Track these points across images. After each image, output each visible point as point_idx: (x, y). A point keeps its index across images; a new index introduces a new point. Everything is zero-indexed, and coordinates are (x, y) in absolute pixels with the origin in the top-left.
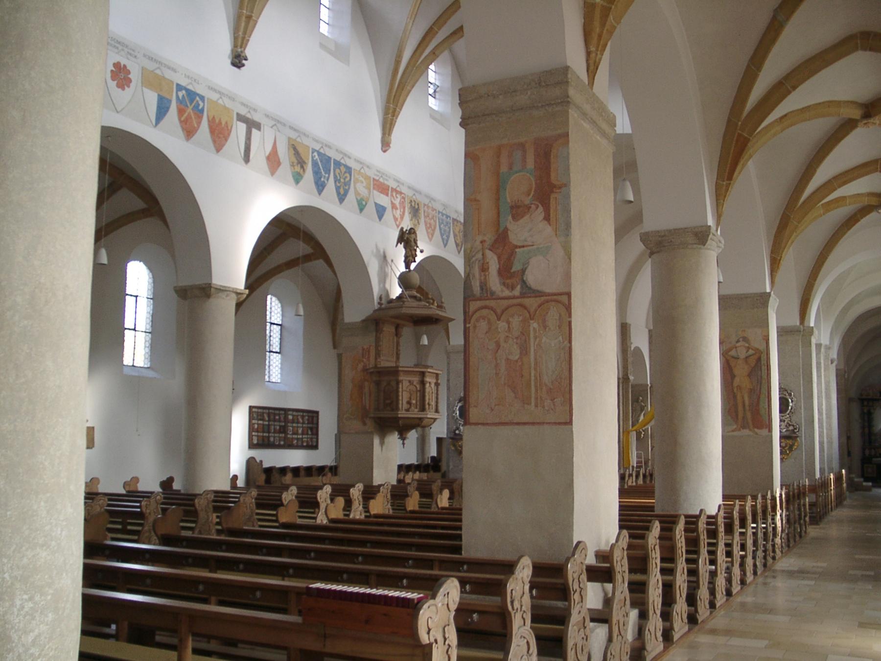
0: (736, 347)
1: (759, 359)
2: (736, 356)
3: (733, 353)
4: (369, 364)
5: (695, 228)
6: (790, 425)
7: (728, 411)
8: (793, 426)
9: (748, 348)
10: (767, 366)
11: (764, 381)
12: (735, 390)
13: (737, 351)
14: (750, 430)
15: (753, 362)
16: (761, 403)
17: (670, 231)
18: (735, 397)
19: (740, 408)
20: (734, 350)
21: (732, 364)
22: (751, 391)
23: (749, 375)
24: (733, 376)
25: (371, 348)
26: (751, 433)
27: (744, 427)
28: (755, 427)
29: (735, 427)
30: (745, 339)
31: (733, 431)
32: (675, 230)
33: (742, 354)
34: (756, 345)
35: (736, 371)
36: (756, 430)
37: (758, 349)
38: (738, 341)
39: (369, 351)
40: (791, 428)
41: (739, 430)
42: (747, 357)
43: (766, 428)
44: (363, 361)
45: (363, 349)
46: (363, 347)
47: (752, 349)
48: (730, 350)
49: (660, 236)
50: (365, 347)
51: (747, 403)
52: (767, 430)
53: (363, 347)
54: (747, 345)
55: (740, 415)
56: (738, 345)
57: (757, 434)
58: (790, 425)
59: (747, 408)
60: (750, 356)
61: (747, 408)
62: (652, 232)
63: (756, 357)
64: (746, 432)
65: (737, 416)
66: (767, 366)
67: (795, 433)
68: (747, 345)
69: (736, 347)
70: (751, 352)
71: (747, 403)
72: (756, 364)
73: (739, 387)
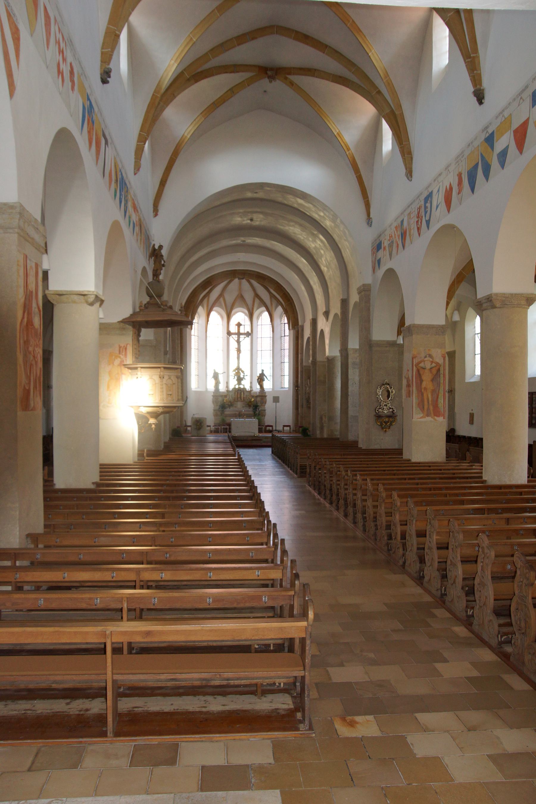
0: (424, 361)
1: (439, 370)
2: (424, 367)
3: (422, 365)
4: (126, 360)
5: (528, 294)
6: (390, 408)
7: (418, 405)
8: (392, 409)
9: (432, 362)
10: (444, 375)
11: (441, 385)
12: (423, 390)
13: (424, 363)
14: (432, 417)
15: (434, 371)
16: (439, 400)
17: (512, 294)
18: (422, 395)
19: (426, 403)
20: (423, 363)
21: (421, 372)
22: (433, 391)
23: (432, 380)
24: (422, 381)
25: (128, 345)
26: (432, 419)
27: (428, 415)
28: (435, 415)
29: (422, 415)
30: (430, 356)
31: (421, 418)
32: (516, 294)
33: (428, 366)
34: (437, 360)
35: (424, 378)
36: (435, 417)
37: (438, 363)
38: (426, 357)
39: (126, 349)
40: (391, 410)
41: (425, 417)
42: (431, 368)
43: (442, 416)
44: (120, 357)
45: (120, 347)
46: (119, 345)
47: (435, 363)
48: (420, 362)
49: (505, 297)
50: (122, 345)
51: (430, 399)
52: (442, 418)
53: (119, 345)
54: (431, 360)
55: (426, 407)
56: (426, 359)
57: (436, 420)
58: (390, 408)
59: (430, 402)
60: (433, 367)
61: (430, 402)
62: (500, 294)
63: (438, 367)
64: (429, 419)
65: (423, 408)
66: (444, 375)
67: (393, 413)
68: (431, 360)
69: (424, 361)
70: (434, 365)
71: (430, 399)
72: (437, 373)
73: (425, 389)
